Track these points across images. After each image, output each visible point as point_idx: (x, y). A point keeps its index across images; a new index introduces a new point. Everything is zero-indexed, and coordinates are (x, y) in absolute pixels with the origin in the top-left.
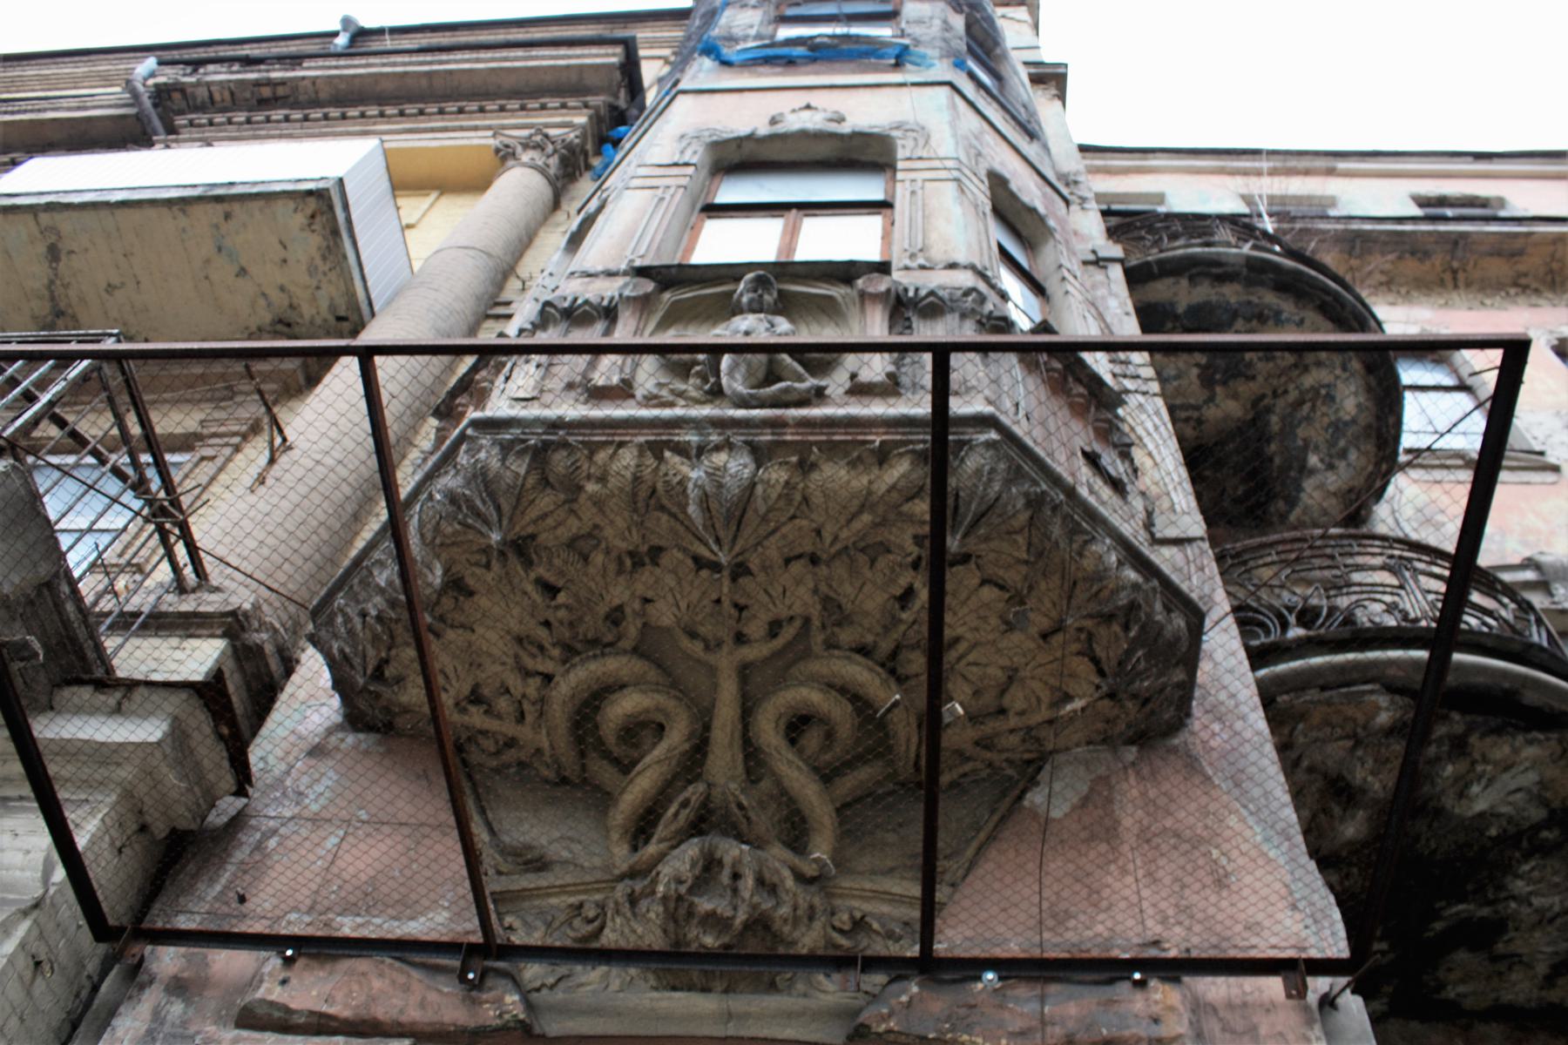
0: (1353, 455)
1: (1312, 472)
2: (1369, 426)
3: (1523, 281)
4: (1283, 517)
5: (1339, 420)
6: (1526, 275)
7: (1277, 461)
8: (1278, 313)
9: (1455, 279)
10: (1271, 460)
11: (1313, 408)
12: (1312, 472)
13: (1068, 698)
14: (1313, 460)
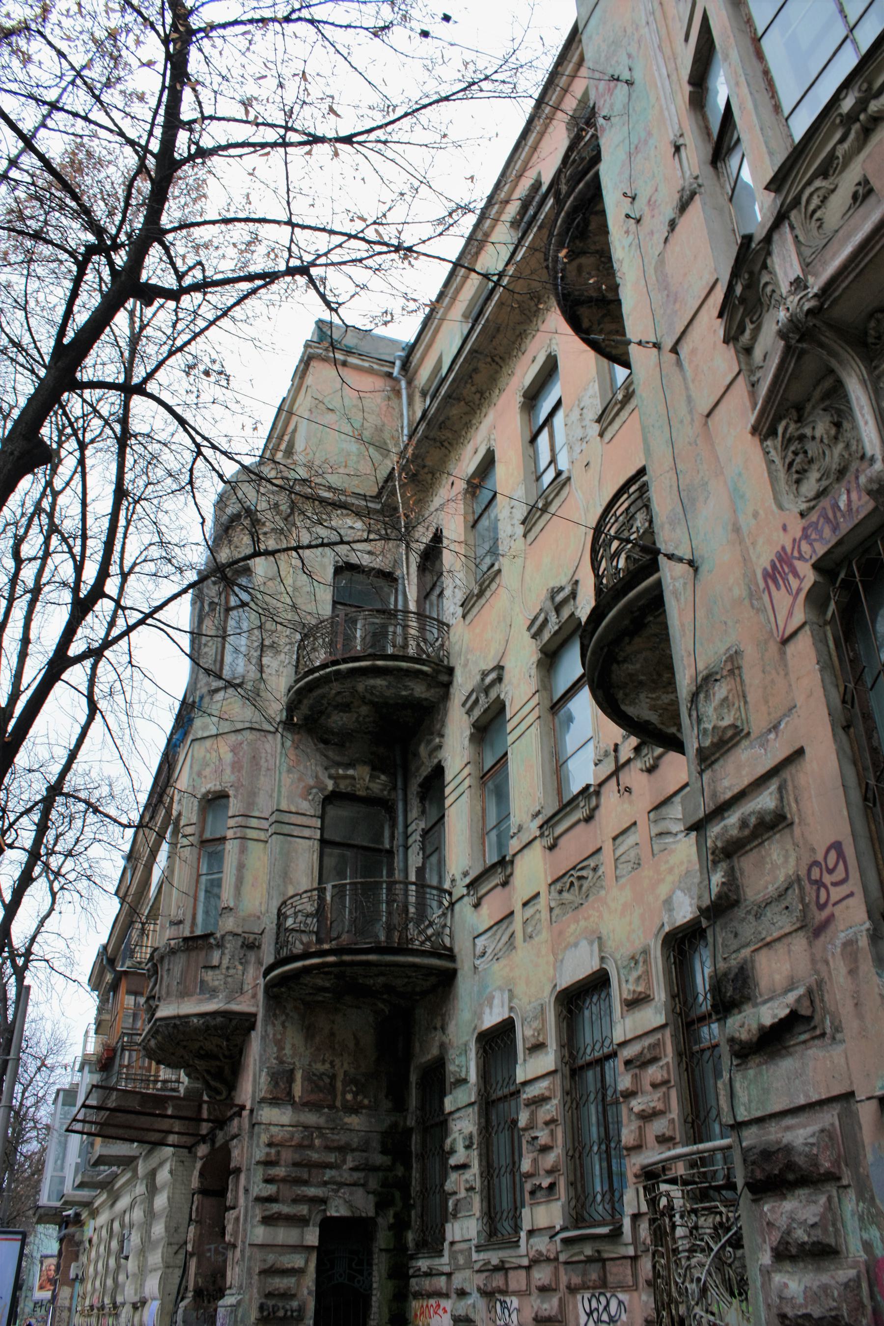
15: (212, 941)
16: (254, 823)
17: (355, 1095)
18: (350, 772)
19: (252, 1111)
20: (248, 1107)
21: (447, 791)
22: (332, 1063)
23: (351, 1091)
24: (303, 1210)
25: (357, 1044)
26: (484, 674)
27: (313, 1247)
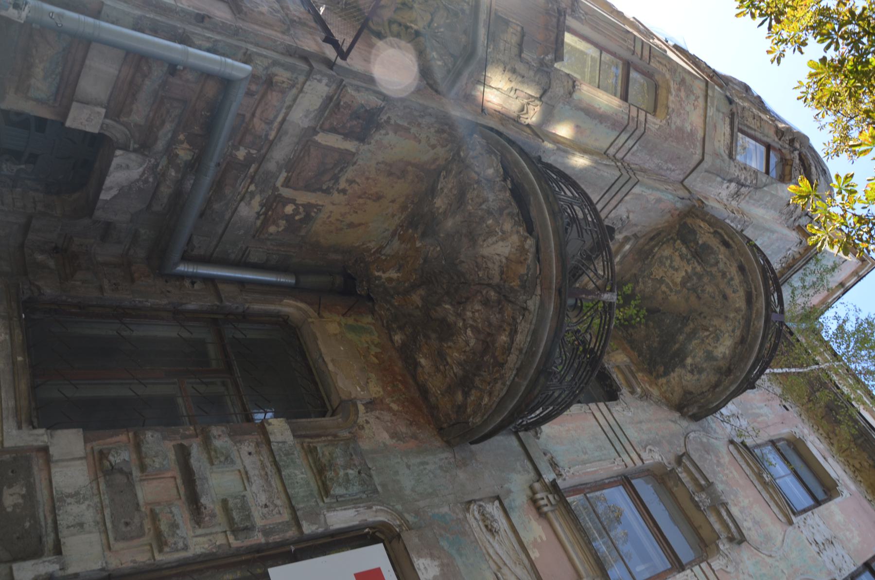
1: (684, 366)
4: (658, 377)
5: (712, 352)
7: (677, 346)
8: (732, 279)
11: (707, 337)
12: (684, 366)
13: (416, 25)
14: (689, 361)
15: (550, 57)
16: (630, 143)
17: (289, 218)
19: (331, 65)
20: (339, 61)
21: (602, 405)
22: (344, 191)
23: (296, 212)
24: (139, 114)
25: (351, 225)
26: (725, 505)
27: (65, 116)
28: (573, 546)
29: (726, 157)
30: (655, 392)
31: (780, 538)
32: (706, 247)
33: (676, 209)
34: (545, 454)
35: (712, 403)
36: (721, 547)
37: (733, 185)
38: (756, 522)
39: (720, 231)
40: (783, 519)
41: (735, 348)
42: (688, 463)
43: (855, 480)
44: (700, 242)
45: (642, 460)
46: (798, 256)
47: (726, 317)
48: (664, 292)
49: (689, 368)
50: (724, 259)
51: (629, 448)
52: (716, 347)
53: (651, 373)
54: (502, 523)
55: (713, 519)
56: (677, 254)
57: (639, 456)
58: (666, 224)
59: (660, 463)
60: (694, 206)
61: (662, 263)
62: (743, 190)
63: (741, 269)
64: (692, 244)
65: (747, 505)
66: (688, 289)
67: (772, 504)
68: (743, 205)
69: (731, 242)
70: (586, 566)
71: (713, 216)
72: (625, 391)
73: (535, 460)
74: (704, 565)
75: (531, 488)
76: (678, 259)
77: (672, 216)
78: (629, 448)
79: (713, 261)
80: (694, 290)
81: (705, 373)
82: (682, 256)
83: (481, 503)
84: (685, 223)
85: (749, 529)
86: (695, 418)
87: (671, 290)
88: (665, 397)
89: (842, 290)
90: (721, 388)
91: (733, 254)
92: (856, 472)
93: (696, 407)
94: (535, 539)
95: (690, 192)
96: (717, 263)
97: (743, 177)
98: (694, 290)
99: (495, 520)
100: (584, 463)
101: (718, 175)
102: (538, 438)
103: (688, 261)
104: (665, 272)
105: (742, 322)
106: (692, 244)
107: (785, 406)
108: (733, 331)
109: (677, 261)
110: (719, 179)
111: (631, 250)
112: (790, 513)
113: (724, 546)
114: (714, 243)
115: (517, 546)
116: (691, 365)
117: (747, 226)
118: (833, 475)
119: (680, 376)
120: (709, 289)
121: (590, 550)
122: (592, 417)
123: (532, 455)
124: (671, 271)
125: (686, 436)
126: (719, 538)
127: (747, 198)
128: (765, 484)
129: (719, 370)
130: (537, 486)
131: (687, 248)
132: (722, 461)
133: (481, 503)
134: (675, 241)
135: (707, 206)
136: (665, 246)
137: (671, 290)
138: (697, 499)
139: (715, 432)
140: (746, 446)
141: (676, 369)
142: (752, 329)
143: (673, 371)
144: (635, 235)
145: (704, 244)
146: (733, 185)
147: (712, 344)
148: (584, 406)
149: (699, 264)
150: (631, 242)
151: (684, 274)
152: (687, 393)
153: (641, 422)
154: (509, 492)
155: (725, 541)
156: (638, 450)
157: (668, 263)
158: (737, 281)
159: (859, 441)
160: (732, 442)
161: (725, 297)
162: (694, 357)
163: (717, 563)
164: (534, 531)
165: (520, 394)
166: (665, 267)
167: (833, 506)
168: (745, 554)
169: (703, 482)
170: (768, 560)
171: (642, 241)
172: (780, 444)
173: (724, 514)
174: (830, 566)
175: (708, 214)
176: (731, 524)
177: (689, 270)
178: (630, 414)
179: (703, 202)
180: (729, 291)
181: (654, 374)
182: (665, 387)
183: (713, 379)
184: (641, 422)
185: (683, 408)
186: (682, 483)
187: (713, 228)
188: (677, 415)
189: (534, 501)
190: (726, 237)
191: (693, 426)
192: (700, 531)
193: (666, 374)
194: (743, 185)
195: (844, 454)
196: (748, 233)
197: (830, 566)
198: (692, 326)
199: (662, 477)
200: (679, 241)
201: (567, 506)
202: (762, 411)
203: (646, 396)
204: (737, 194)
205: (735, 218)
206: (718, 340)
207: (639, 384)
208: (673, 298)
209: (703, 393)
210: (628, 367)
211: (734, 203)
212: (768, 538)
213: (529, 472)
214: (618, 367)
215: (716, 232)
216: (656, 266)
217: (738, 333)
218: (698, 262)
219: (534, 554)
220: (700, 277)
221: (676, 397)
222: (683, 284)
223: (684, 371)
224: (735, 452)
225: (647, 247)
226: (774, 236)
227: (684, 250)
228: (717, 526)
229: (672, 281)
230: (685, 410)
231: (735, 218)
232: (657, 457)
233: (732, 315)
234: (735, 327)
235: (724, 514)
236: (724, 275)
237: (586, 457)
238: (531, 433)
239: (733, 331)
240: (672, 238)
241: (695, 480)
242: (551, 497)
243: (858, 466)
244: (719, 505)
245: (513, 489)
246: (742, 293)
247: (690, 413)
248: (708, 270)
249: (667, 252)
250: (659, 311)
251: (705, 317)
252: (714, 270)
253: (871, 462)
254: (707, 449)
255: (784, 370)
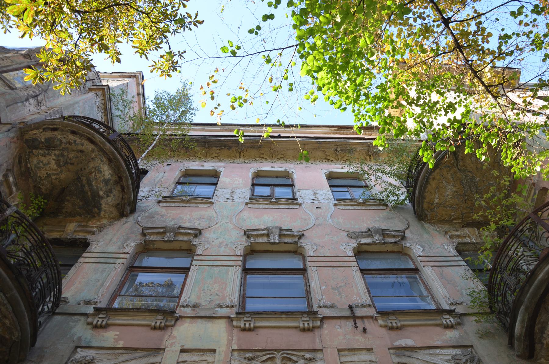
0: (114, 192)
1: (102, 198)
2: (116, 181)
3: (262, 156)
4: (99, 215)
6: (263, 154)
7: (89, 193)
8: (75, 141)
9: (240, 155)
10: (87, 193)
11: (95, 175)
12: (102, 198)
14: (101, 193)
18: (14, 189)
21: (85, 255)
26: (180, 227)
28: (133, 320)
29: (10, 91)
30: (104, 221)
31: (214, 213)
32: (48, 140)
33: (13, 138)
34: (79, 304)
35: (130, 197)
36: (195, 243)
37: (31, 100)
38: (199, 219)
39: (45, 127)
40: (208, 205)
41: (111, 166)
42: (148, 231)
43: (221, 161)
44: (43, 141)
45: (127, 253)
46: (103, 102)
47: (92, 159)
48: (56, 179)
49: (105, 196)
50: (62, 136)
51: (117, 256)
52: (104, 175)
53: (94, 216)
54: (91, 353)
55: (181, 238)
56: (40, 157)
57: (124, 253)
58: (18, 150)
59: (137, 245)
60: (20, 128)
61: (39, 168)
62: (39, 98)
63: (73, 133)
64: (41, 145)
65: (187, 217)
66: (64, 166)
67: (199, 205)
68: (49, 104)
69: (55, 126)
70: (148, 318)
71: (34, 124)
72: (89, 237)
73: (77, 312)
74: (195, 258)
75: (88, 324)
76: (43, 158)
77: (15, 143)
78: (117, 256)
79: (58, 143)
80: (66, 163)
81: (113, 190)
82: (43, 155)
83: (71, 359)
84: (27, 140)
85: (199, 224)
86: (133, 211)
87: (57, 174)
88: (112, 218)
89: (141, 97)
90: (126, 188)
91: (62, 131)
92: (218, 157)
93: (127, 207)
94: (114, 339)
95: (10, 124)
96: (61, 141)
97: (31, 92)
98: (66, 163)
99: (87, 356)
100: (102, 285)
101: (17, 103)
102: (69, 302)
103: (48, 154)
104: (46, 170)
105: (100, 153)
106: (41, 145)
107: (168, 165)
108: (102, 161)
109: (44, 160)
110: (19, 104)
111: (14, 178)
112: (208, 200)
113: (196, 242)
114: (49, 134)
115: (109, 352)
116: (104, 193)
117: (61, 111)
118: (211, 168)
119: (106, 204)
120: (71, 155)
121: (142, 312)
122: (85, 264)
123: (73, 312)
124: (48, 167)
125: (137, 222)
126: (191, 242)
127: (47, 100)
128: (188, 202)
129: (116, 183)
130: (90, 320)
131: (41, 149)
132: (162, 213)
133: (71, 359)
134: (32, 152)
135: (28, 122)
136: (30, 159)
137: (57, 174)
138: (166, 239)
139: (148, 206)
140: (165, 197)
141: (101, 202)
142: (107, 152)
143: (101, 205)
144: (8, 170)
145: (46, 139)
146: (31, 100)
147: (101, 176)
148: (77, 265)
149: (55, 150)
150: (10, 175)
151: (54, 162)
152: (117, 206)
153: (111, 240)
154: (80, 338)
155: (194, 239)
156: (122, 252)
157: (41, 165)
158: (78, 140)
159: (207, 146)
160: (159, 202)
161: (82, 151)
162: (101, 189)
163: (199, 251)
164: (110, 337)
165: (19, 298)
166: (43, 168)
167: (222, 179)
168: (207, 235)
169: (162, 230)
170: (217, 226)
171: (16, 169)
172: (181, 181)
173: (183, 231)
174: (241, 200)
175: (31, 125)
176: (190, 231)
177: (54, 158)
178: (102, 243)
179: (23, 122)
180: (80, 147)
181: (96, 215)
182: (107, 215)
183: (119, 188)
184: (111, 240)
185: (123, 213)
186: (154, 241)
187: (40, 128)
188: (124, 219)
189: (96, 327)
190: (51, 127)
191: (136, 215)
192: (182, 248)
193: (100, 209)
194: (37, 96)
195: (207, 156)
196: (66, 114)
197: (241, 200)
198: (84, 178)
199: (146, 248)
200: (34, 151)
201: (116, 310)
202: (160, 176)
203: (101, 228)
204: (39, 103)
205: (50, 114)
206: (101, 172)
207: (92, 227)
208: (62, 176)
209: (122, 198)
210: (80, 226)
211: (43, 108)
212: (210, 219)
213: (80, 320)
214: (75, 231)
215: (44, 129)
216: (38, 172)
217: (104, 159)
218: (53, 150)
219: (121, 344)
220: (62, 155)
221: (116, 213)
222: (59, 165)
223: (105, 200)
224: (165, 204)
225: (23, 169)
226: (81, 104)
227: (41, 152)
228: (186, 238)
229: (53, 170)
230: (125, 213)
231: (50, 114)
232: (133, 244)
233: (93, 155)
234: (100, 158)
235: (183, 231)
236: (70, 143)
237: (101, 282)
238: (62, 305)
239: (102, 161)
240: (29, 153)
241: (158, 233)
242: (101, 316)
243: (216, 155)
244: (177, 231)
245: (80, 335)
246: (86, 142)
247: (129, 212)
248: (61, 148)
249: (35, 161)
250: (64, 188)
251: (85, 169)
252: (63, 145)
253: (218, 148)
254: (151, 216)
255: (146, 152)
